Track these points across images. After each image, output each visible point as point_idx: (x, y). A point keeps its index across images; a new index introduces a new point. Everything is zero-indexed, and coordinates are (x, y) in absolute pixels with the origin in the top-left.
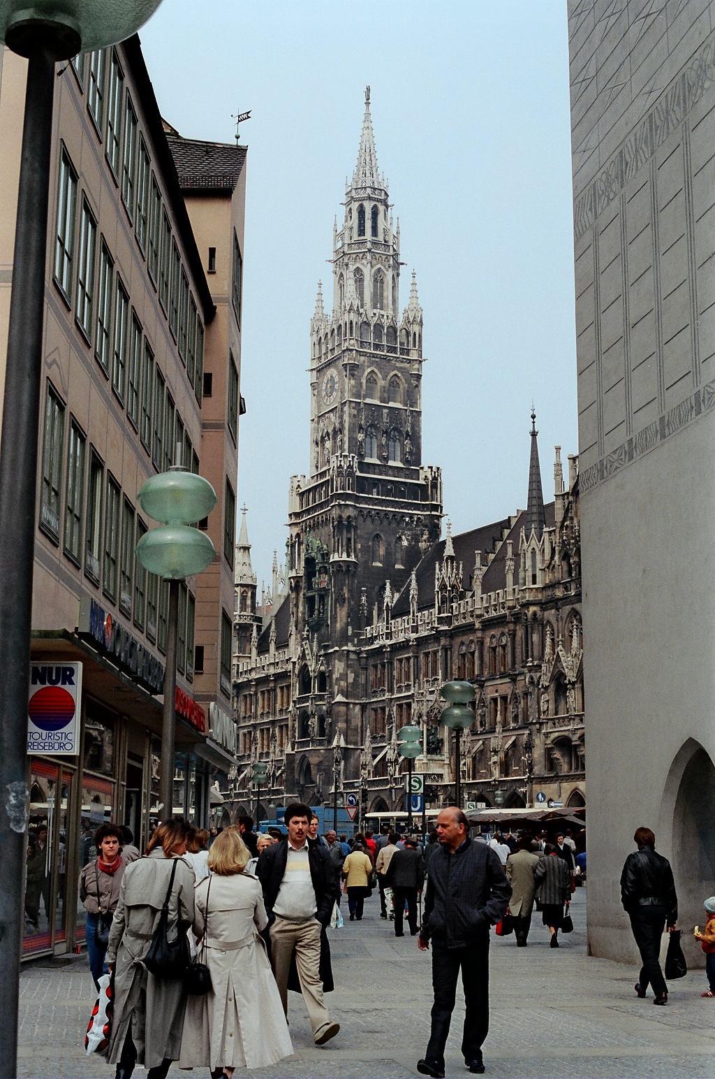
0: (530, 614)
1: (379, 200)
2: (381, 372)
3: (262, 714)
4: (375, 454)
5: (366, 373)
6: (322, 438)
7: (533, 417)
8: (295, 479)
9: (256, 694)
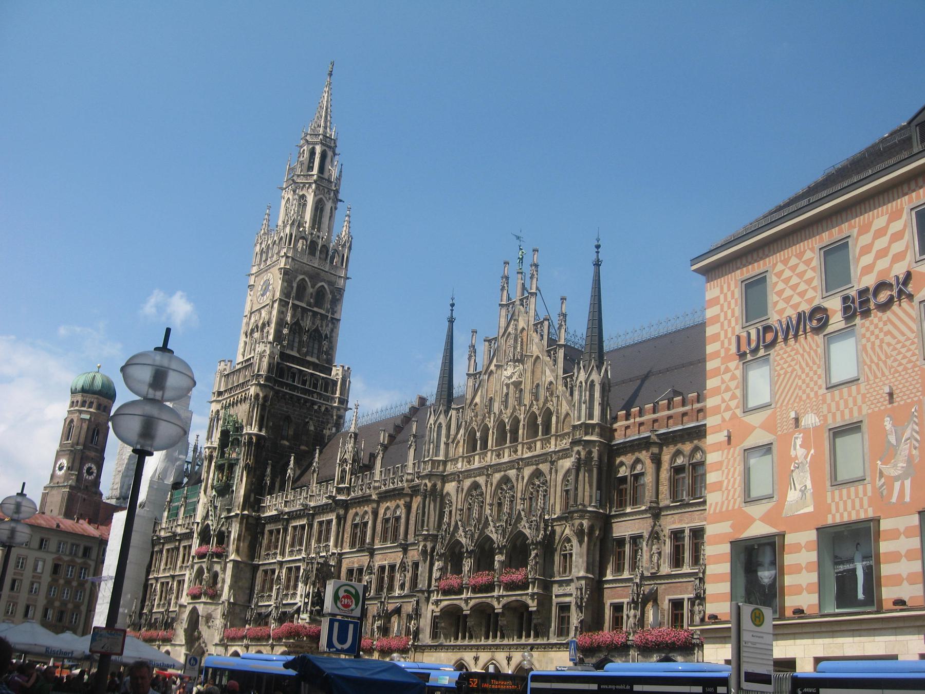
0: (429, 485)
1: (330, 147)
3: (165, 569)
4: (295, 349)
5: (298, 279)
6: (252, 331)
7: (452, 305)
8: (222, 364)
9: (161, 551)
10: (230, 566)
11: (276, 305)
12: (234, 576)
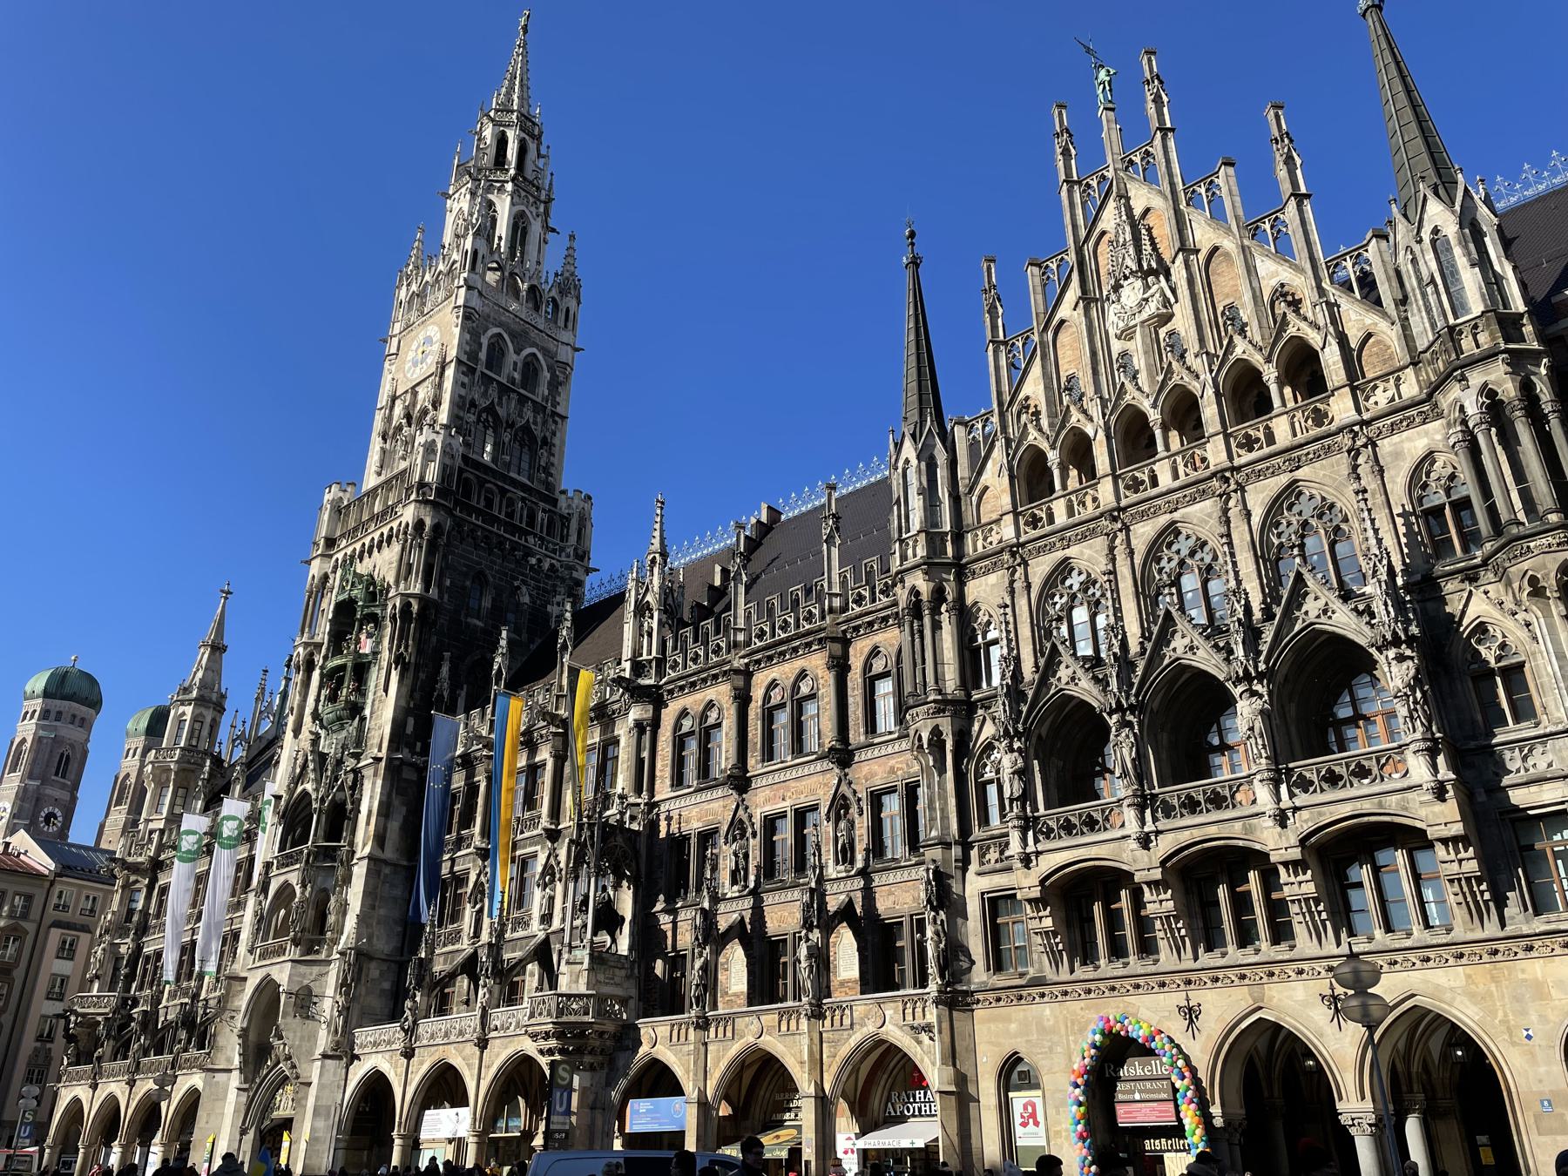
1: (532, 136)
10: (360, 871)
11: (450, 372)
12: (367, 893)
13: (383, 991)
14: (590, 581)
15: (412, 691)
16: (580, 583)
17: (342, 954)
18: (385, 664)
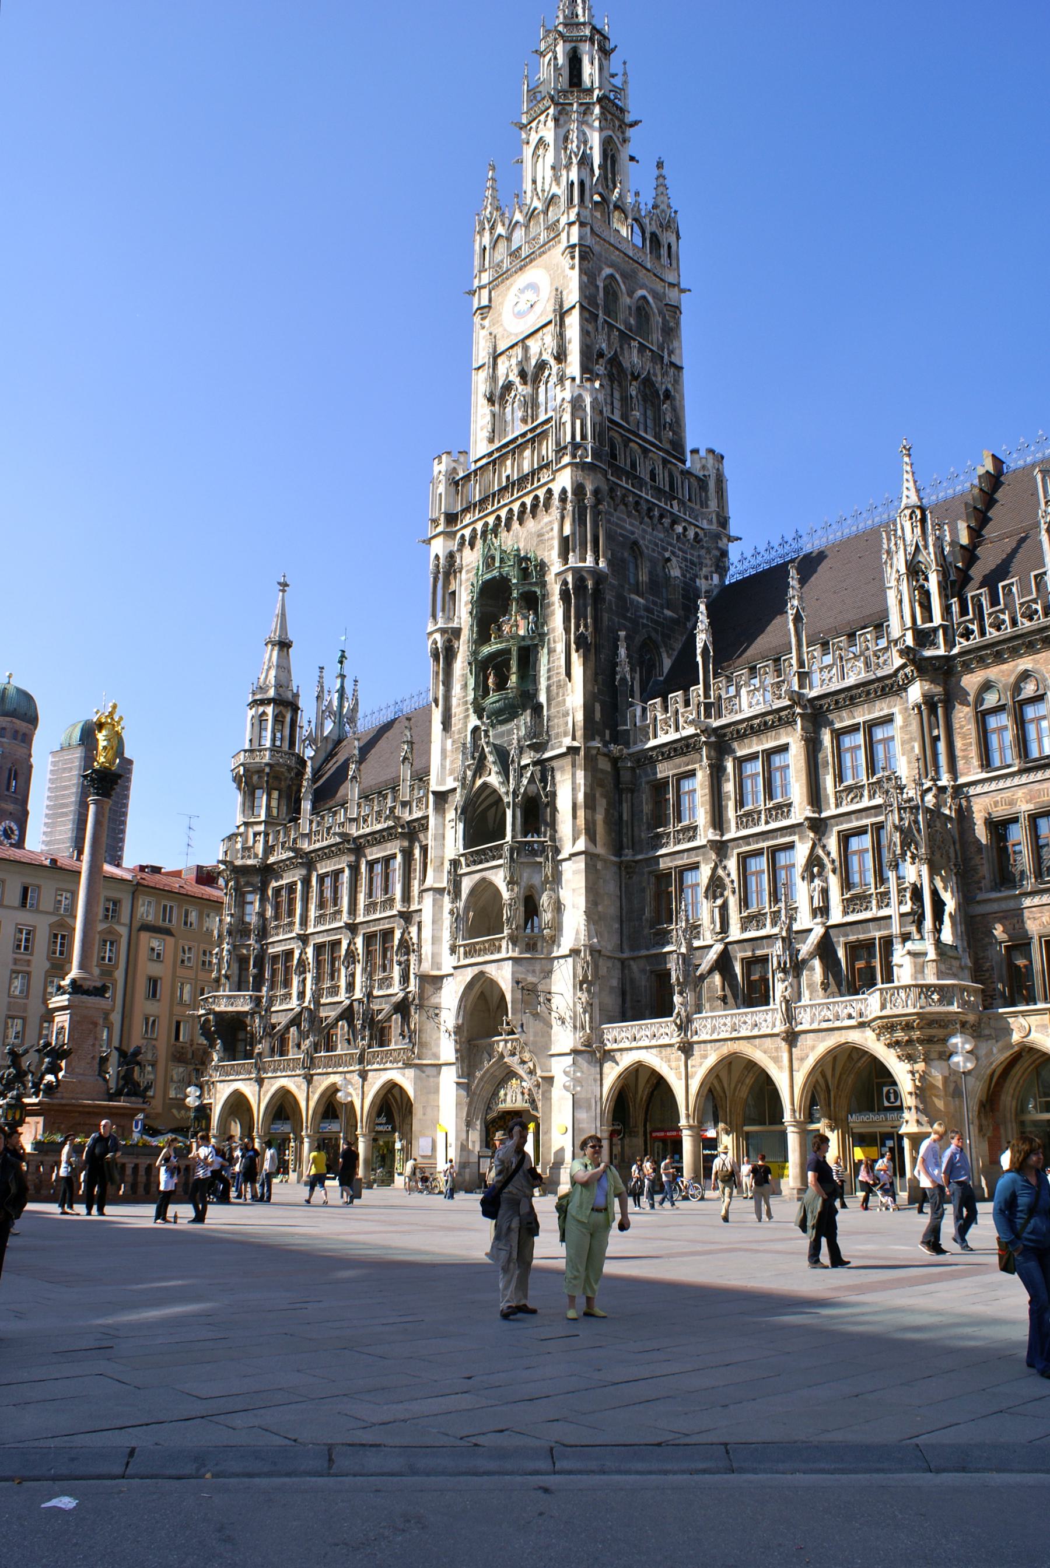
2: (624, 283)
13: (612, 988)
14: (734, 551)
15: (596, 674)
16: (724, 554)
17: (575, 952)
18: (560, 647)
